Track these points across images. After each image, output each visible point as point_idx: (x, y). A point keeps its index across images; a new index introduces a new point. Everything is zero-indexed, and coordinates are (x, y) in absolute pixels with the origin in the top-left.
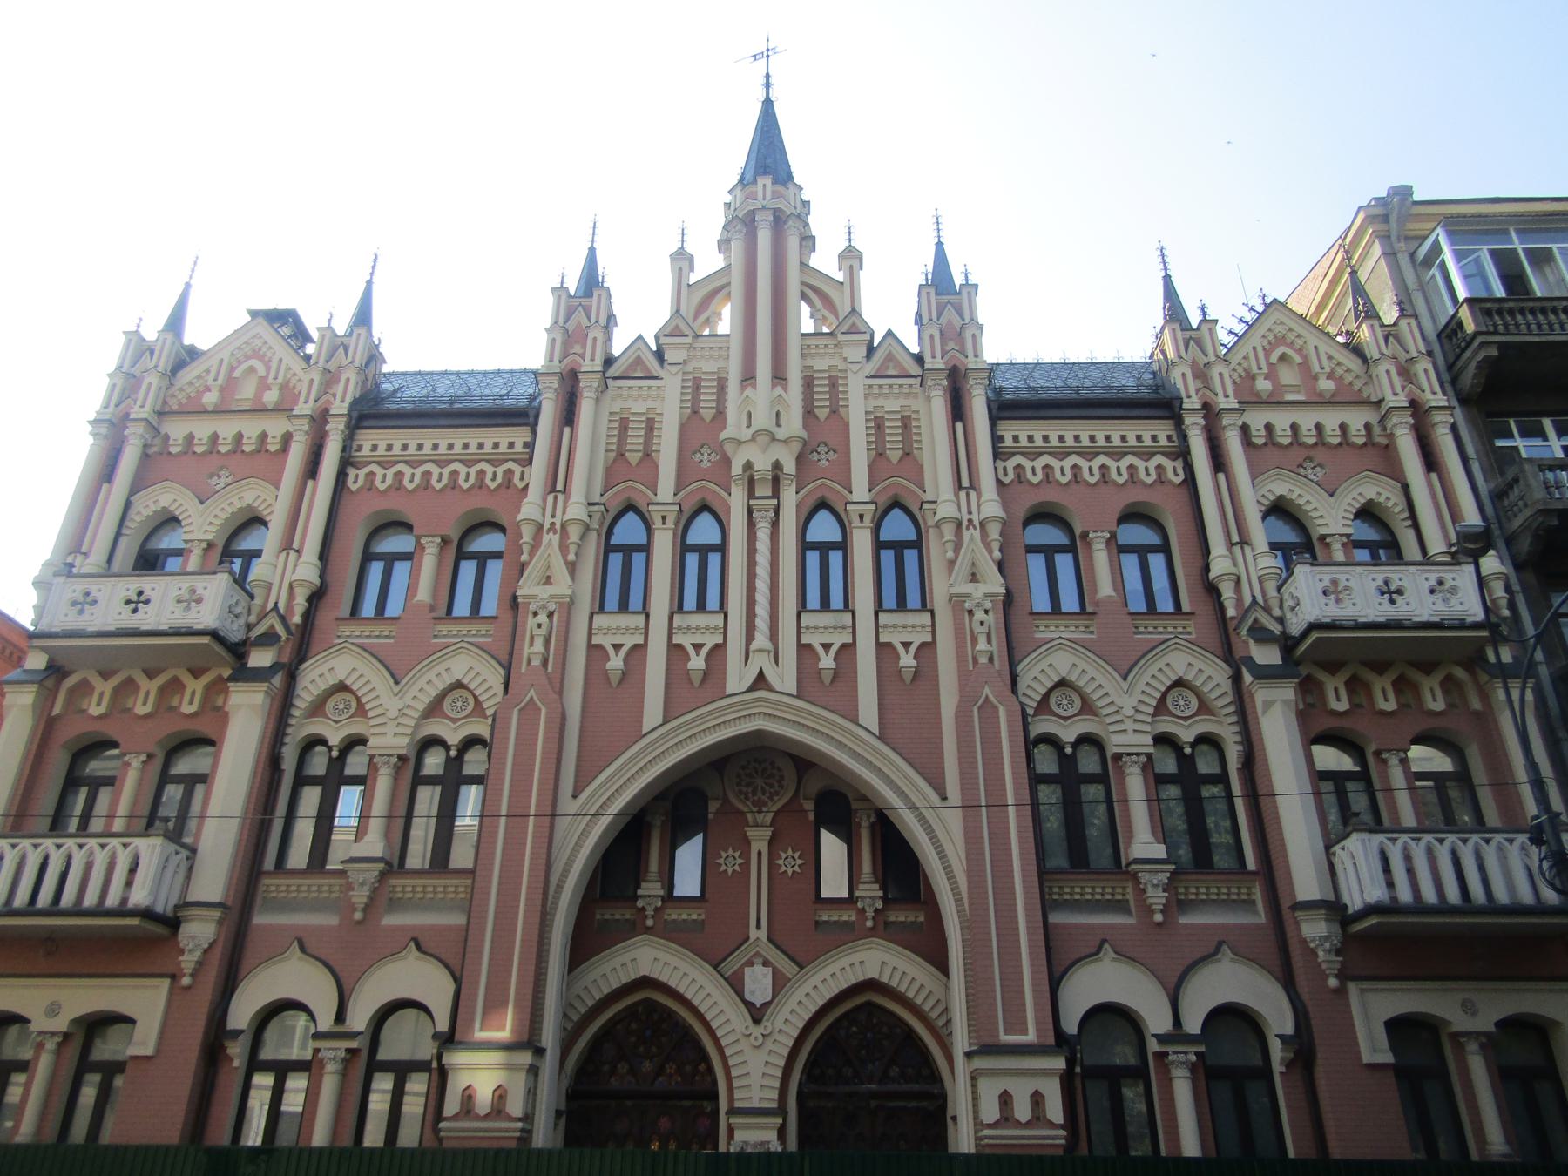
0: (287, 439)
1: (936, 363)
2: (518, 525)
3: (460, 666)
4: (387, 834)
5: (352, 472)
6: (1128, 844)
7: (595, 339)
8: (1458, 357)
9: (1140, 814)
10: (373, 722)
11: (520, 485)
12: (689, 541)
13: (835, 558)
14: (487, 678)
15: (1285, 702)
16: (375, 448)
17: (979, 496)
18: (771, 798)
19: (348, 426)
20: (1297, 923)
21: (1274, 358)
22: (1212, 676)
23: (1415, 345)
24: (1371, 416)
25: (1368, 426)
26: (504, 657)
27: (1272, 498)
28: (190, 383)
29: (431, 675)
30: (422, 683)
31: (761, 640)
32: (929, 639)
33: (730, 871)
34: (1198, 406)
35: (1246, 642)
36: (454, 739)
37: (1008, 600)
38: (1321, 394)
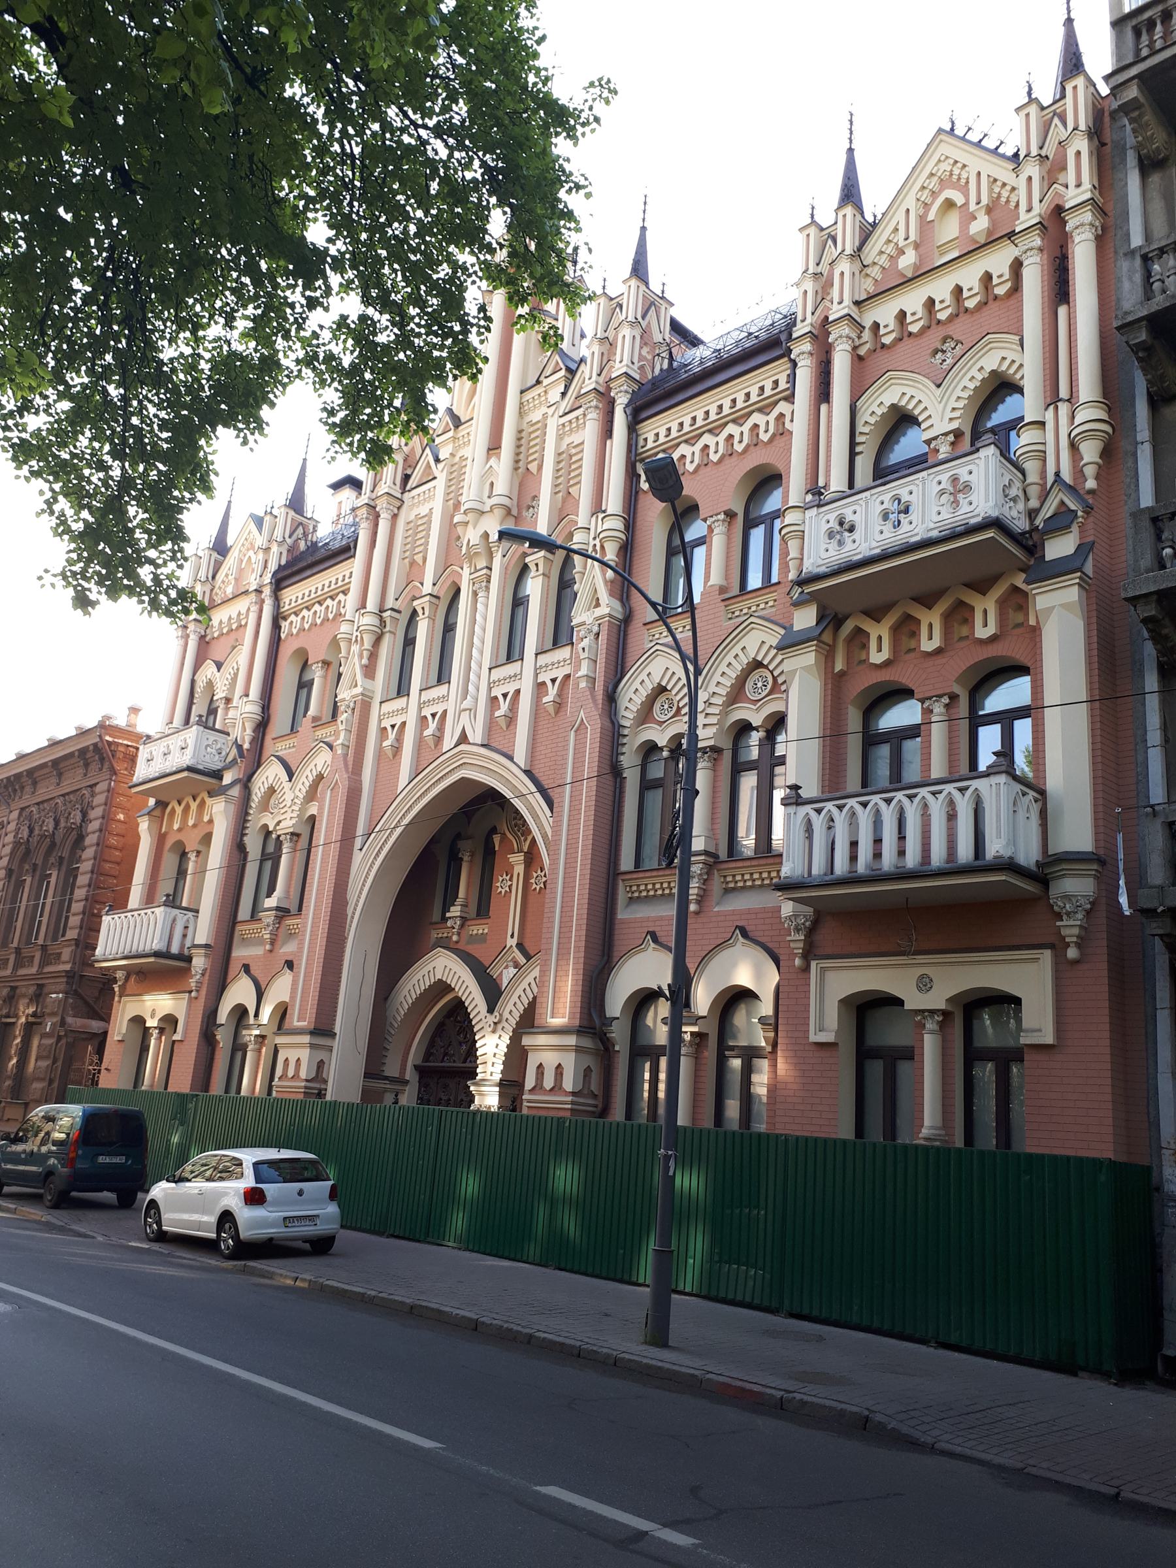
29: (308, 772)
30: (303, 779)
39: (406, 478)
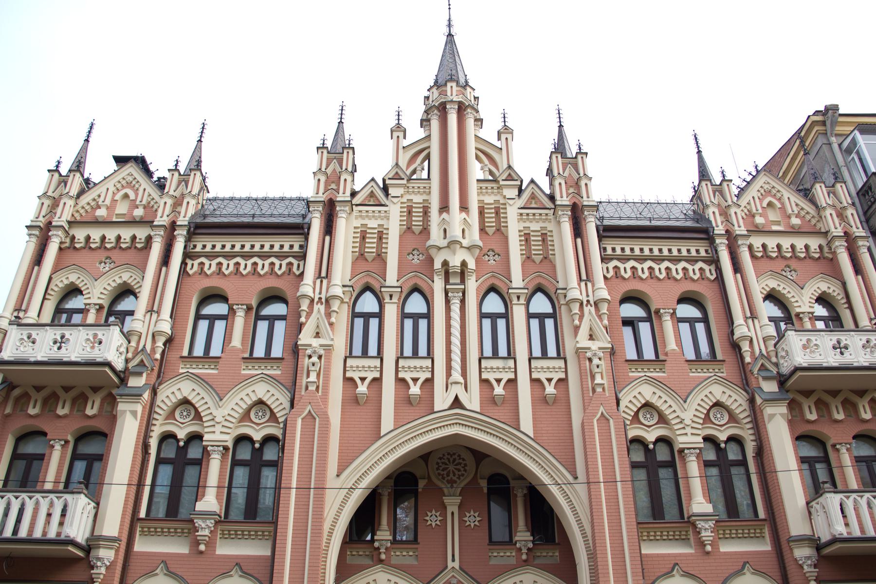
0: (149, 239)
1: (563, 199)
2: (298, 298)
3: (261, 390)
4: (218, 497)
5: (189, 262)
6: (689, 505)
7: (345, 180)
8: (870, 207)
9: (697, 485)
10: (205, 424)
11: (298, 273)
12: (407, 310)
13: (501, 323)
14: (278, 399)
15: (782, 415)
16: (204, 247)
17: (593, 286)
18: (459, 478)
19: (189, 231)
20: (791, 550)
21: (765, 205)
22: (736, 400)
23: (846, 200)
24: (823, 242)
25: (820, 247)
26: (288, 382)
27: (768, 289)
28: (88, 204)
31: (456, 376)
32: (563, 376)
33: (434, 524)
34: (723, 232)
35: (757, 378)
36: (257, 436)
37: (612, 352)
38: (793, 227)
39: (354, 194)
